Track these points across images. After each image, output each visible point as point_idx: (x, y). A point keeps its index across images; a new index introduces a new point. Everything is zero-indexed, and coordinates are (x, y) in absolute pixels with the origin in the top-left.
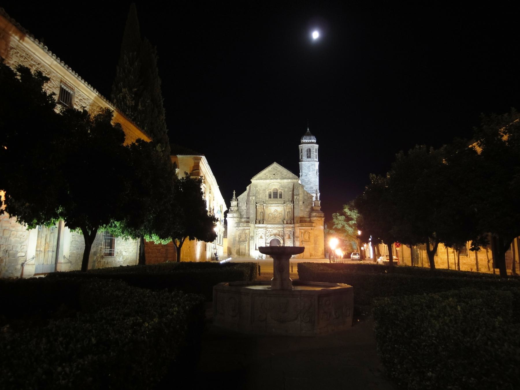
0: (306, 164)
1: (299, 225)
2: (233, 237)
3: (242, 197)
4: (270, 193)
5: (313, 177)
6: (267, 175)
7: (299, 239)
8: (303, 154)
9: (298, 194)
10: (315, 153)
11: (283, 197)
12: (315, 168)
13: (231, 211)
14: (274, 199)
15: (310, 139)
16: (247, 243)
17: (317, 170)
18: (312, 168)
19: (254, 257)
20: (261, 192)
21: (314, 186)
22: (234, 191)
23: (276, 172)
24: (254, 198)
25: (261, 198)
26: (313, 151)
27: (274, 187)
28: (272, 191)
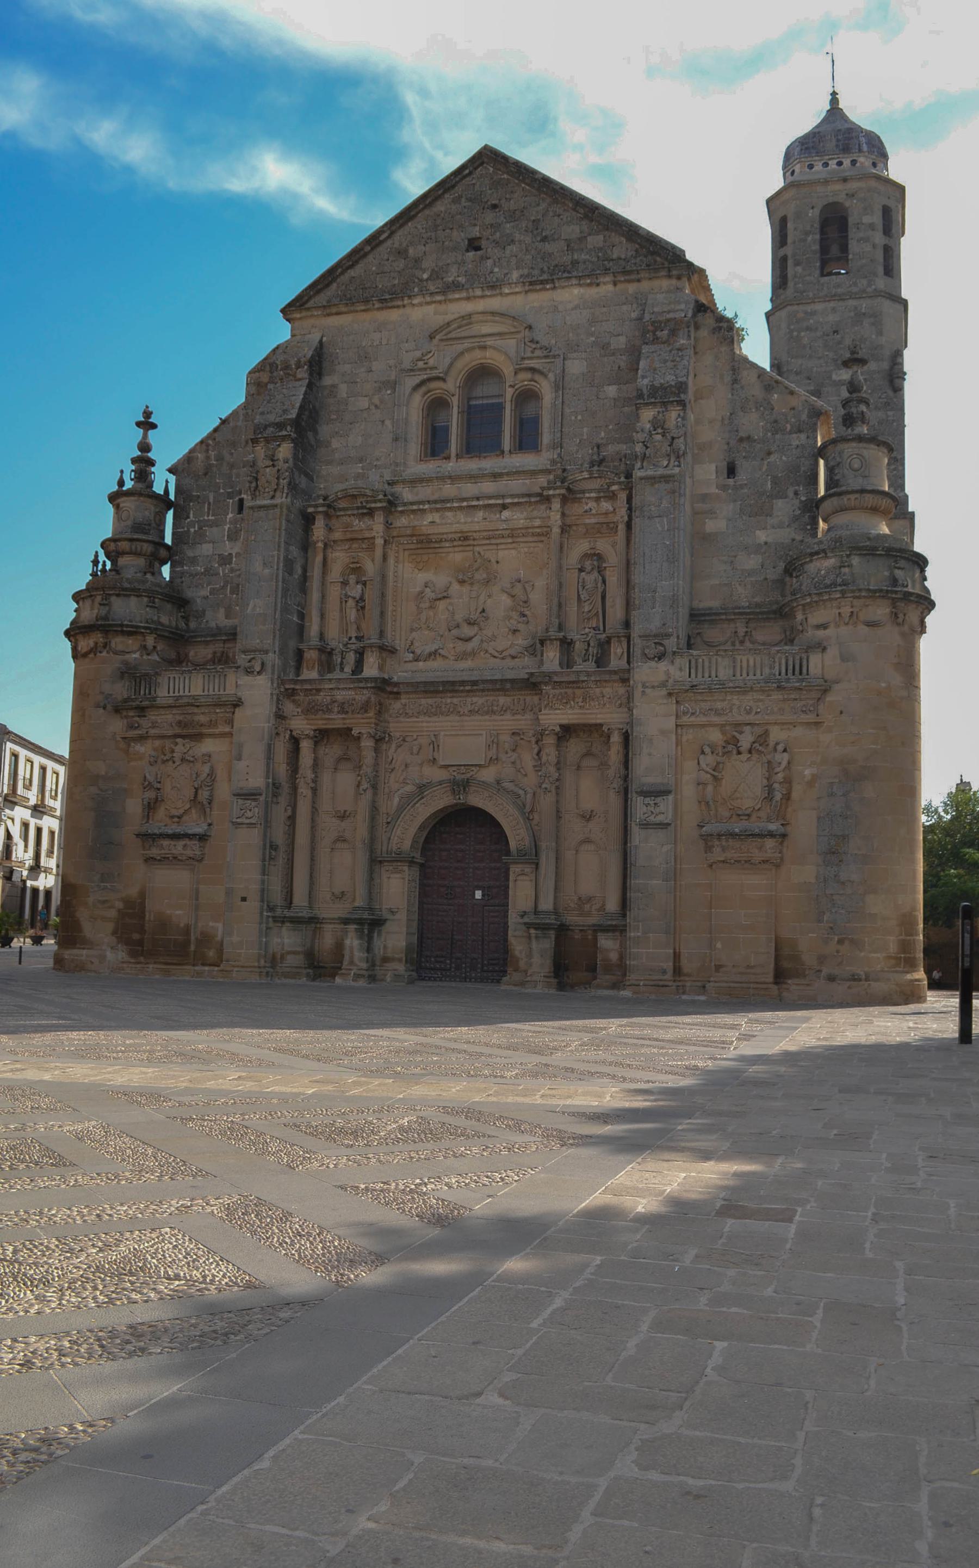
0: (813, 313)
1: (672, 670)
2: (93, 790)
3: (208, 458)
6: (417, 261)
7: (665, 806)
11: (546, 439)
14: (471, 465)
20: (364, 403)
23: (495, 227)
24: (285, 451)
25: (361, 460)
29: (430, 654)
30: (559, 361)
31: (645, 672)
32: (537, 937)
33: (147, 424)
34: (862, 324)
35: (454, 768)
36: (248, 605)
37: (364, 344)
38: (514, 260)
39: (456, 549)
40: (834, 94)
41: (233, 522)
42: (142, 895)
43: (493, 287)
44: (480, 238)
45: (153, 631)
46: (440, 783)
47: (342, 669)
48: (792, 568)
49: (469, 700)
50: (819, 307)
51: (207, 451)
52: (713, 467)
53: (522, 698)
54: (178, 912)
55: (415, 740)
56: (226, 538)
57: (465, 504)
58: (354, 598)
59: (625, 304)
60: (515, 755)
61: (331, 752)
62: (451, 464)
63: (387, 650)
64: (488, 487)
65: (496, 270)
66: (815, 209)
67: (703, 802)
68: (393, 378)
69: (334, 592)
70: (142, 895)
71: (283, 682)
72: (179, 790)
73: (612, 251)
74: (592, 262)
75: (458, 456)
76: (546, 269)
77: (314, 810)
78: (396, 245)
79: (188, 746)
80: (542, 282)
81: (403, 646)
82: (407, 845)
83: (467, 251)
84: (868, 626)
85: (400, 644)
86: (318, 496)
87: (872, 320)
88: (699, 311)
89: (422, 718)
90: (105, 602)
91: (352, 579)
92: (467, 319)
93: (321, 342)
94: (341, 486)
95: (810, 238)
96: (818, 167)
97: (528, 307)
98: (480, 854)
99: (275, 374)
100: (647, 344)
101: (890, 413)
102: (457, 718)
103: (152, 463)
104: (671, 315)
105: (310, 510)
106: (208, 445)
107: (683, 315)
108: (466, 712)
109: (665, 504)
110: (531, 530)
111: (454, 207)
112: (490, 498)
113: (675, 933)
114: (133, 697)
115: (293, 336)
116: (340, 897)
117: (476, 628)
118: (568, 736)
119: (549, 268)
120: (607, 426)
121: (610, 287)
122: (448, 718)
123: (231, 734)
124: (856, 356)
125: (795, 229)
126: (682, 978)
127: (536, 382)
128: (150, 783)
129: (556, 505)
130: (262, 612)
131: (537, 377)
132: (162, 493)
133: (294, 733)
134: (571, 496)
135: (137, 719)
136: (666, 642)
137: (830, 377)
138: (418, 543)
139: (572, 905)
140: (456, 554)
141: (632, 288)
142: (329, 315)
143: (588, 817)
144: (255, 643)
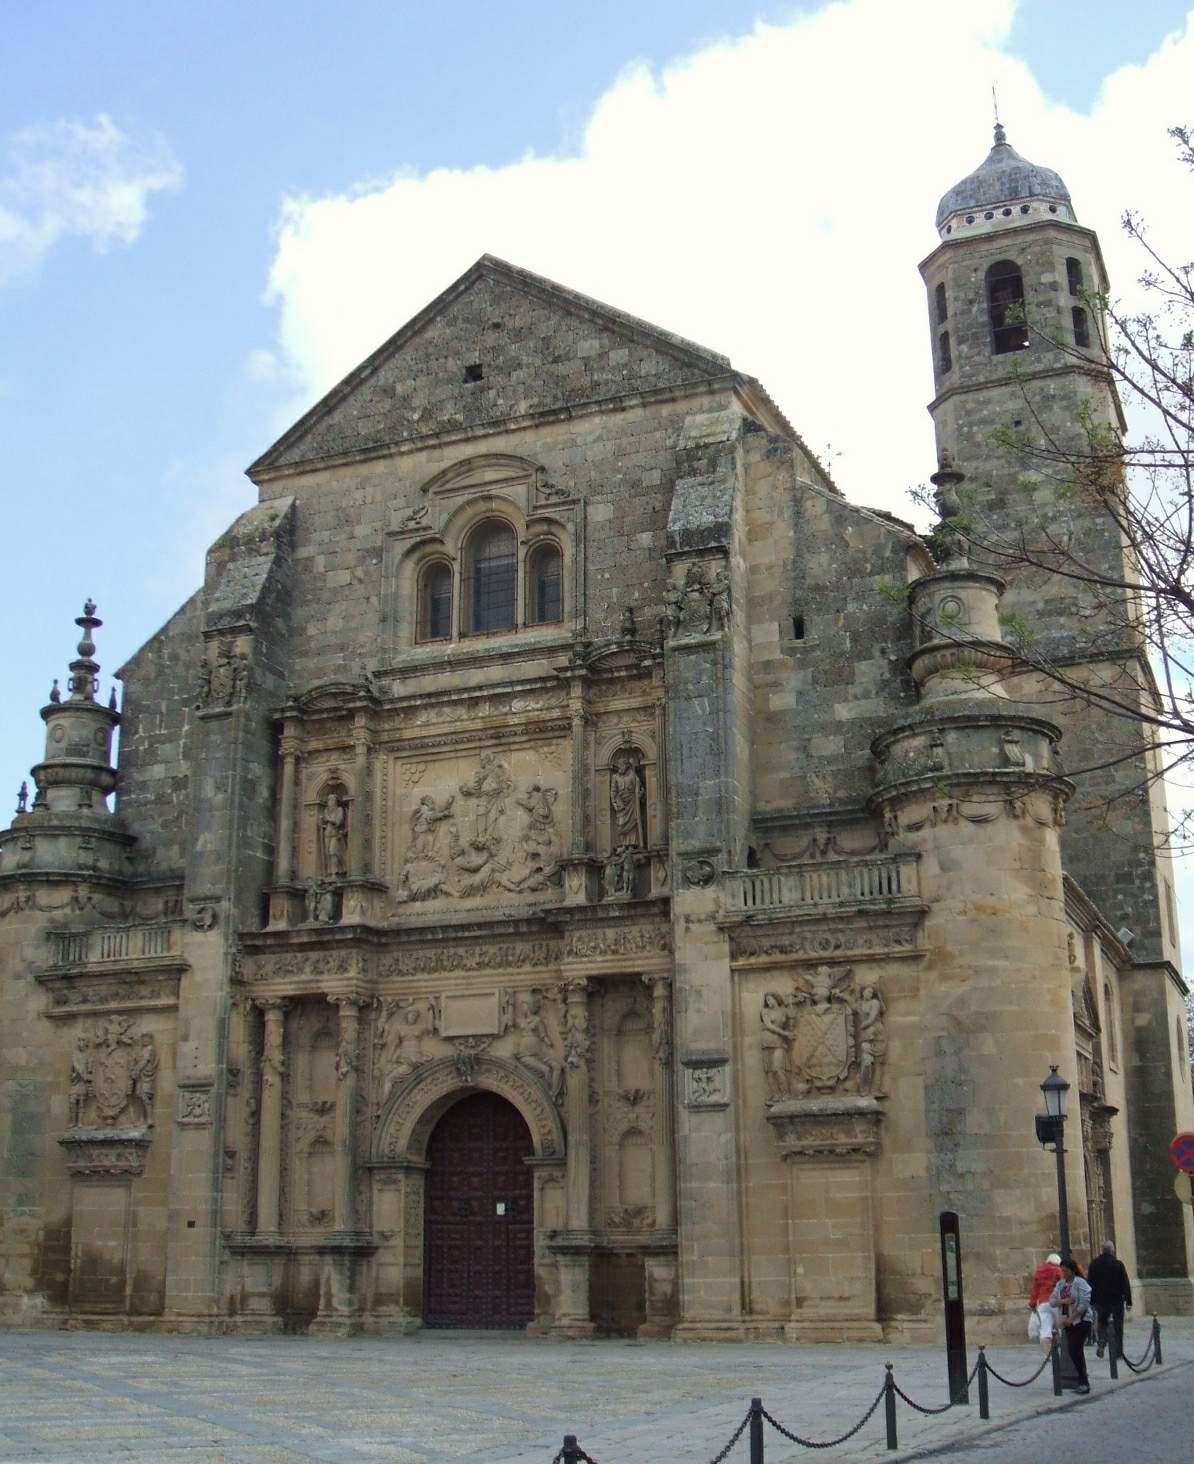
2: (11, 1085)
3: (160, 657)
5: (1062, 506)
7: (723, 1077)
9: (708, 519)
15: (1014, 195)
20: (344, 577)
23: (497, 350)
24: (242, 645)
25: (342, 649)
29: (429, 891)
30: (579, 507)
31: (690, 901)
32: (567, 1266)
33: (89, 622)
34: (1050, 408)
35: (461, 1041)
36: (197, 839)
38: (521, 389)
39: (460, 754)
40: (999, 127)
41: (190, 734)
42: (68, 1223)
43: (495, 423)
44: (480, 366)
45: (85, 879)
46: (442, 1061)
47: (316, 918)
48: (879, 750)
49: (478, 949)
50: (995, 393)
51: (159, 650)
52: (775, 626)
53: (544, 943)
54: (112, 1244)
55: (412, 1004)
56: (181, 757)
57: (465, 696)
58: (333, 824)
59: (658, 430)
60: (537, 1019)
61: (311, 1024)
62: (452, 646)
63: (375, 889)
64: (496, 672)
65: (500, 402)
66: (979, 273)
67: (769, 1072)
68: (379, 543)
69: (310, 819)
70: (68, 1223)
71: (242, 936)
72: (113, 1082)
73: (639, 366)
74: (615, 382)
75: (462, 636)
76: (560, 395)
77: (286, 1102)
78: (381, 382)
79: (125, 1025)
80: (554, 412)
81: (395, 882)
82: (403, 1143)
83: (466, 381)
84: (974, 821)
85: (390, 879)
86: (288, 697)
87: (1064, 403)
88: (749, 431)
89: (419, 976)
90: (28, 845)
92: (466, 465)
93: (293, 506)
94: (316, 683)
95: (975, 309)
96: (980, 218)
97: (539, 444)
98: (501, 1154)
99: (236, 550)
100: (681, 477)
101: (1099, 520)
102: (463, 973)
103: (95, 668)
104: (710, 440)
105: (277, 716)
106: (161, 642)
107: (725, 439)
108: (474, 965)
109: (705, 680)
110: (550, 724)
111: (448, 331)
112: (497, 685)
113: (742, 1252)
114: (60, 964)
115: (262, 501)
116: (321, 1217)
117: (485, 855)
118: (602, 991)
119: (563, 394)
120: (641, 584)
121: (639, 411)
122: (452, 974)
123: (174, 1009)
124: (949, 470)
125: (956, 299)
126: (754, 1317)
127: (552, 534)
128: (78, 1075)
129: (577, 691)
130: (213, 848)
131: (554, 529)
132: (107, 706)
133: (258, 1002)
134: (596, 677)
135: (65, 991)
136: (713, 860)
138: (411, 748)
139: (617, 1220)
140: (460, 760)
141: (666, 410)
143: (634, 1099)
144: (204, 888)
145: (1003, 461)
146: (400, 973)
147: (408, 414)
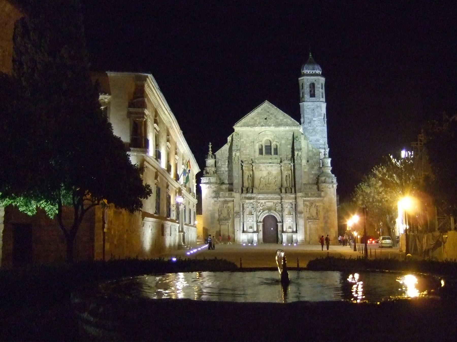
0: (309, 105)
4: (261, 147)
5: (319, 124)
8: (305, 90)
10: (321, 90)
12: (322, 112)
13: (207, 173)
15: (314, 70)
16: (230, 221)
17: (324, 114)
18: (318, 112)
19: (241, 243)
20: (248, 145)
21: (320, 137)
22: (210, 144)
25: (249, 155)
26: (318, 86)
27: (266, 138)
28: (263, 143)
34: (318, 108)
36: (234, 181)
37: (248, 134)
66: (309, 83)
68: (253, 141)
82: (262, 220)
91: (249, 176)
95: (308, 89)
101: (324, 128)
111: (262, 111)
137: (312, 119)
142: (242, 128)
145: (310, 116)
146: (260, 200)
147: (256, 122)
